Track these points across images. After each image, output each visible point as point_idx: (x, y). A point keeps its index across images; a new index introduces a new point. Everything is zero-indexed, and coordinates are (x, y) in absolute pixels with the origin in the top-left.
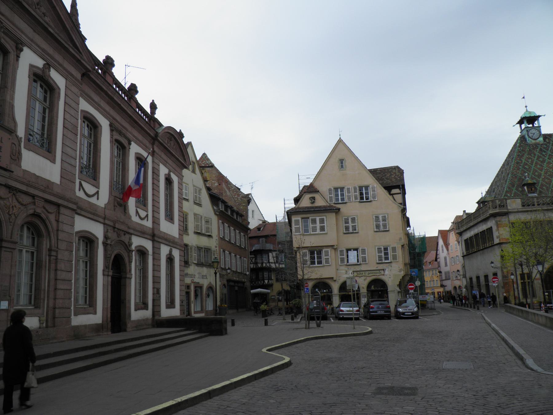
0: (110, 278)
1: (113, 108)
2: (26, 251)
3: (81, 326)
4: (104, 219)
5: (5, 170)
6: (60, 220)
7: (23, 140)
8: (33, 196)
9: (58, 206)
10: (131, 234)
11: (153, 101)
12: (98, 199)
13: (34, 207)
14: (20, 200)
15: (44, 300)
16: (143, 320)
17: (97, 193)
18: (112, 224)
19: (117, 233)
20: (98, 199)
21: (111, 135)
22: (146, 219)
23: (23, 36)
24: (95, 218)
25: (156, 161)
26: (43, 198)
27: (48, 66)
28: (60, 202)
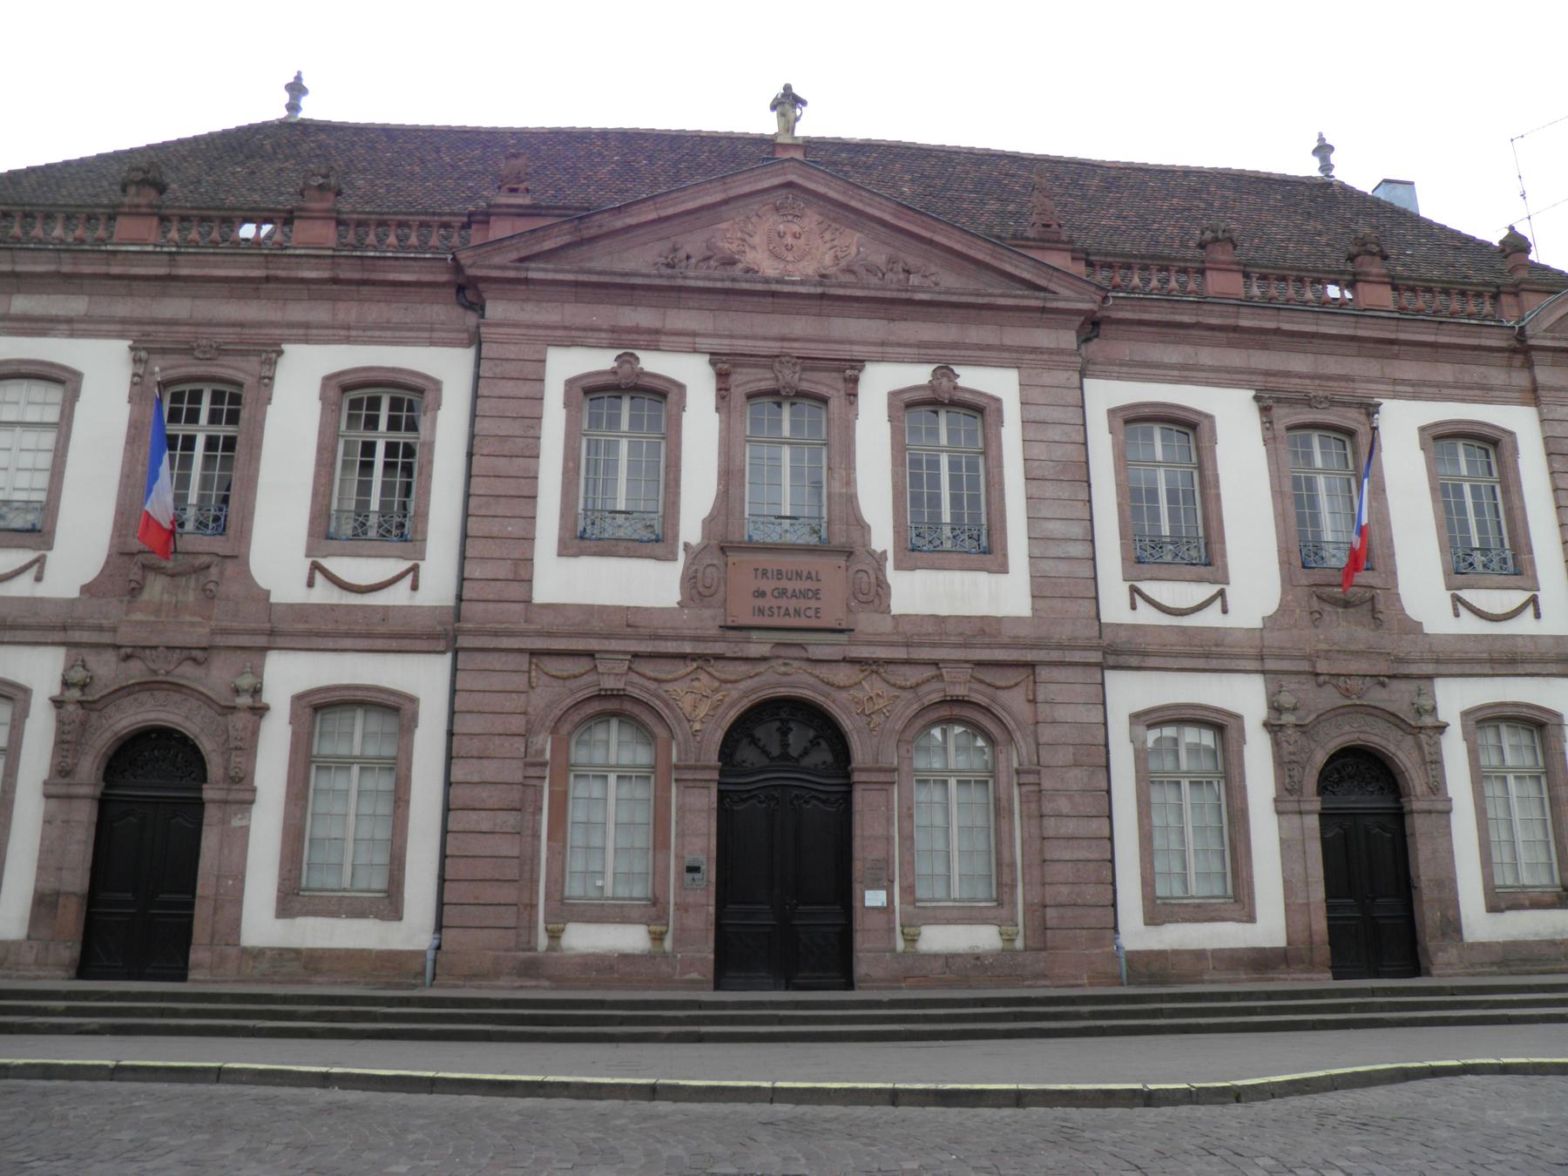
0: (1313, 822)
1: (1264, 347)
2: (959, 782)
3: (1176, 953)
4: (1262, 658)
5: (841, 631)
6: (1040, 698)
7: (890, 556)
8: (935, 663)
9: (1031, 666)
10: (1430, 677)
11: (1511, 228)
12: (1225, 611)
13: (939, 685)
14: (892, 679)
15: (1014, 886)
16: (1553, 943)
17: (1222, 593)
18: (1305, 666)
19: (1337, 687)
20: (1225, 611)
21: (1263, 423)
22: (1530, 610)
23: (856, 348)
24: (1214, 663)
26: (967, 662)
27: (944, 372)
28: (1030, 656)
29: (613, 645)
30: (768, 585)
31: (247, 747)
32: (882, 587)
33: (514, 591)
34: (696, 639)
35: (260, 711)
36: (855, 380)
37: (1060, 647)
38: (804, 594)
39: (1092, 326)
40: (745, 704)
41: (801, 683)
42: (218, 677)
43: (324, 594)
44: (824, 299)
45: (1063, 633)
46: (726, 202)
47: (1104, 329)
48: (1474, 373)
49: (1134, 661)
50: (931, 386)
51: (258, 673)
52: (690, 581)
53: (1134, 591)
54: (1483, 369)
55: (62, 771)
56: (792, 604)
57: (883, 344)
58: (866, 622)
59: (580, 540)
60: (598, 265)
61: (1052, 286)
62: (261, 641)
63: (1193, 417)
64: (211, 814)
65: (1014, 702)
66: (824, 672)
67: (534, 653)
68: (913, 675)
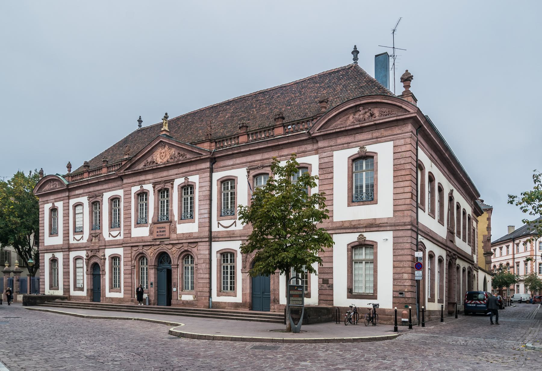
1: (250, 155)
8: (182, 243)
9: (197, 242)
17: (235, 222)
24: (232, 239)
25: (324, 155)
27: (186, 178)
28: (197, 240)
29: (140, 244)
30: (159, 230)
31: (104, 265)
32: (175, 227)
33: (129, 235)
34: (150, 242)
35: (105, 259)
36: (172, 184)
37: (201, 238)
38: (163, 231)
39: (213, 160)
40: (157, 253)
41: (164, 248)
42: (100, 254)
43: (111, 238)
44: (167, 167)
45: (202, 235)
46: (153, 148)
47: (217, 160)
48: (303, 148)
49: (217, 239)
50: (184, 183)
51: (104, 252)
52: (150, 230)
53: (219, 223)
54: (306, 146)
55: (87, 270)
56: (162, 233)
57: (176, 174)
58: (173, 236)
59: (138, 224)
60: (136, 168)
61: (202, 153)
62: (104, 247)
63: (233, 178)
64: (101, 276)
65: (194, 250)
66: (167, 246)
67: (132, 246)
68: (180, 246)
